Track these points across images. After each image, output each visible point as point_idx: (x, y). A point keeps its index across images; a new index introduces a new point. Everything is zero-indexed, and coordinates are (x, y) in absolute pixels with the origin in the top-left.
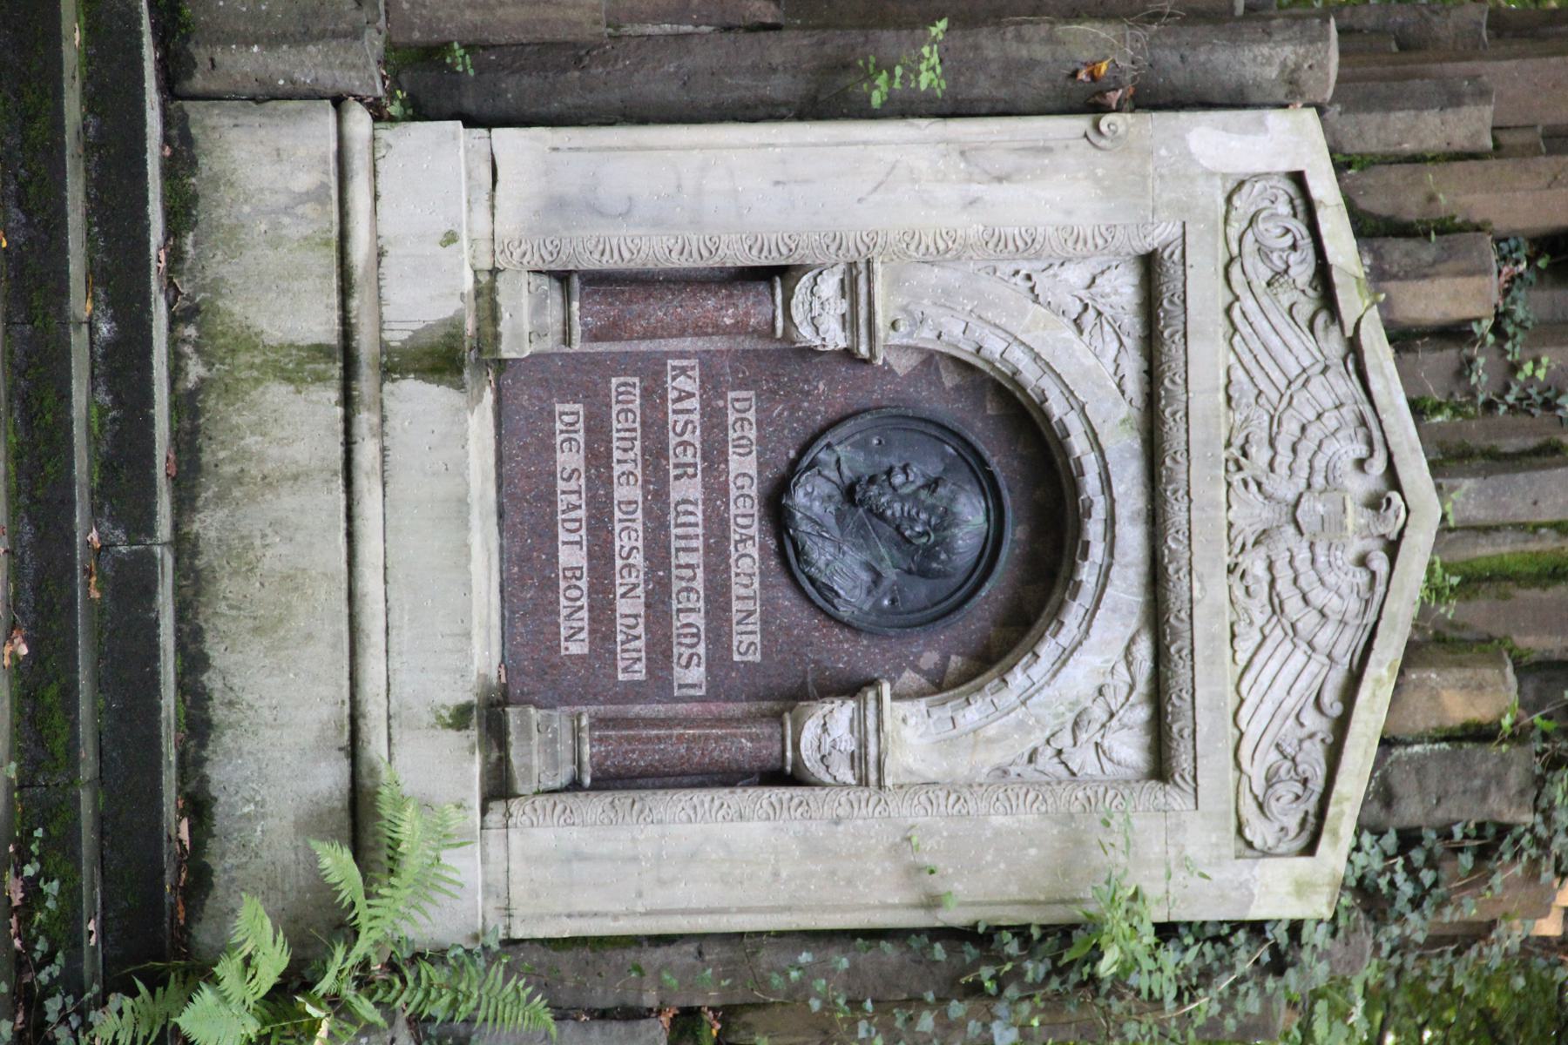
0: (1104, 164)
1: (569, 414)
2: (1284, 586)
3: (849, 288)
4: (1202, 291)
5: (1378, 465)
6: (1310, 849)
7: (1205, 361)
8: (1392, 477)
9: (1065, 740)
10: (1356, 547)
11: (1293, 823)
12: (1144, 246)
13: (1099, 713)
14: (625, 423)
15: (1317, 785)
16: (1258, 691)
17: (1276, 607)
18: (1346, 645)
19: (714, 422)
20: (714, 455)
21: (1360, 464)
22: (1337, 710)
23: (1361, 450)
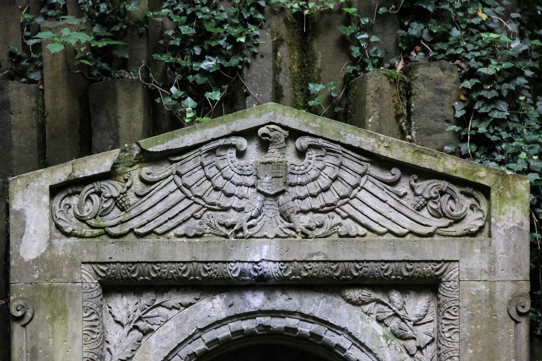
0: (43, 314)
2: (317, 203)
5: (242, 142)
6: (486, 191)
8: (250, 134)
9: (412, 345)
10: (291, 158)
11: (468, 202)
12: (97, 290)
13: (394, 323)
15: (444, 184)
16: (383, 219)
21: (241, 154)
22: (396, 171)
23: (231, 154)
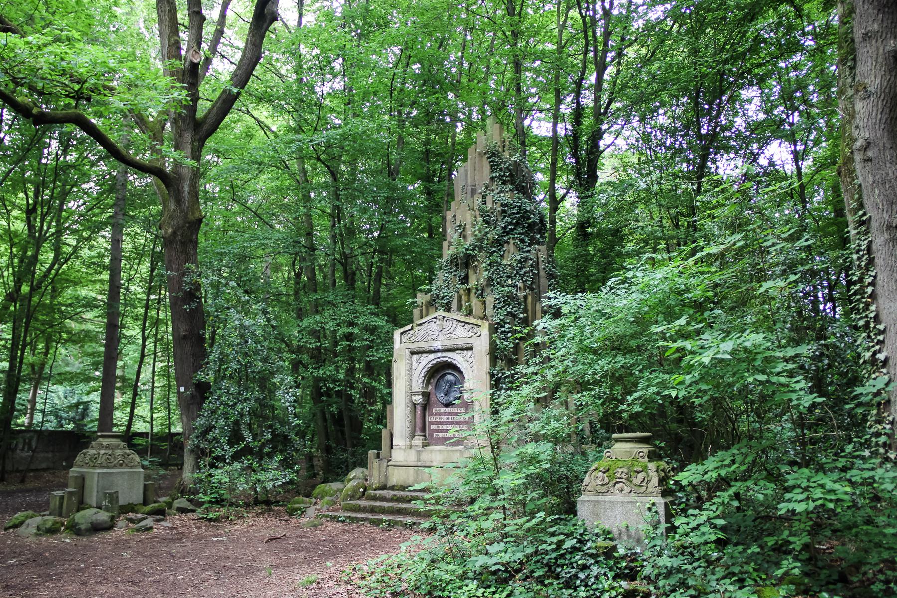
1: (436, 435)
3: (414, 395)
4: (416, 345)
7: (422, 345)
14: (436, 427)
16: (461, 335)
17: (451, 333)
18: (455, 323)
19: (436, 414)
20: (440, 414)
